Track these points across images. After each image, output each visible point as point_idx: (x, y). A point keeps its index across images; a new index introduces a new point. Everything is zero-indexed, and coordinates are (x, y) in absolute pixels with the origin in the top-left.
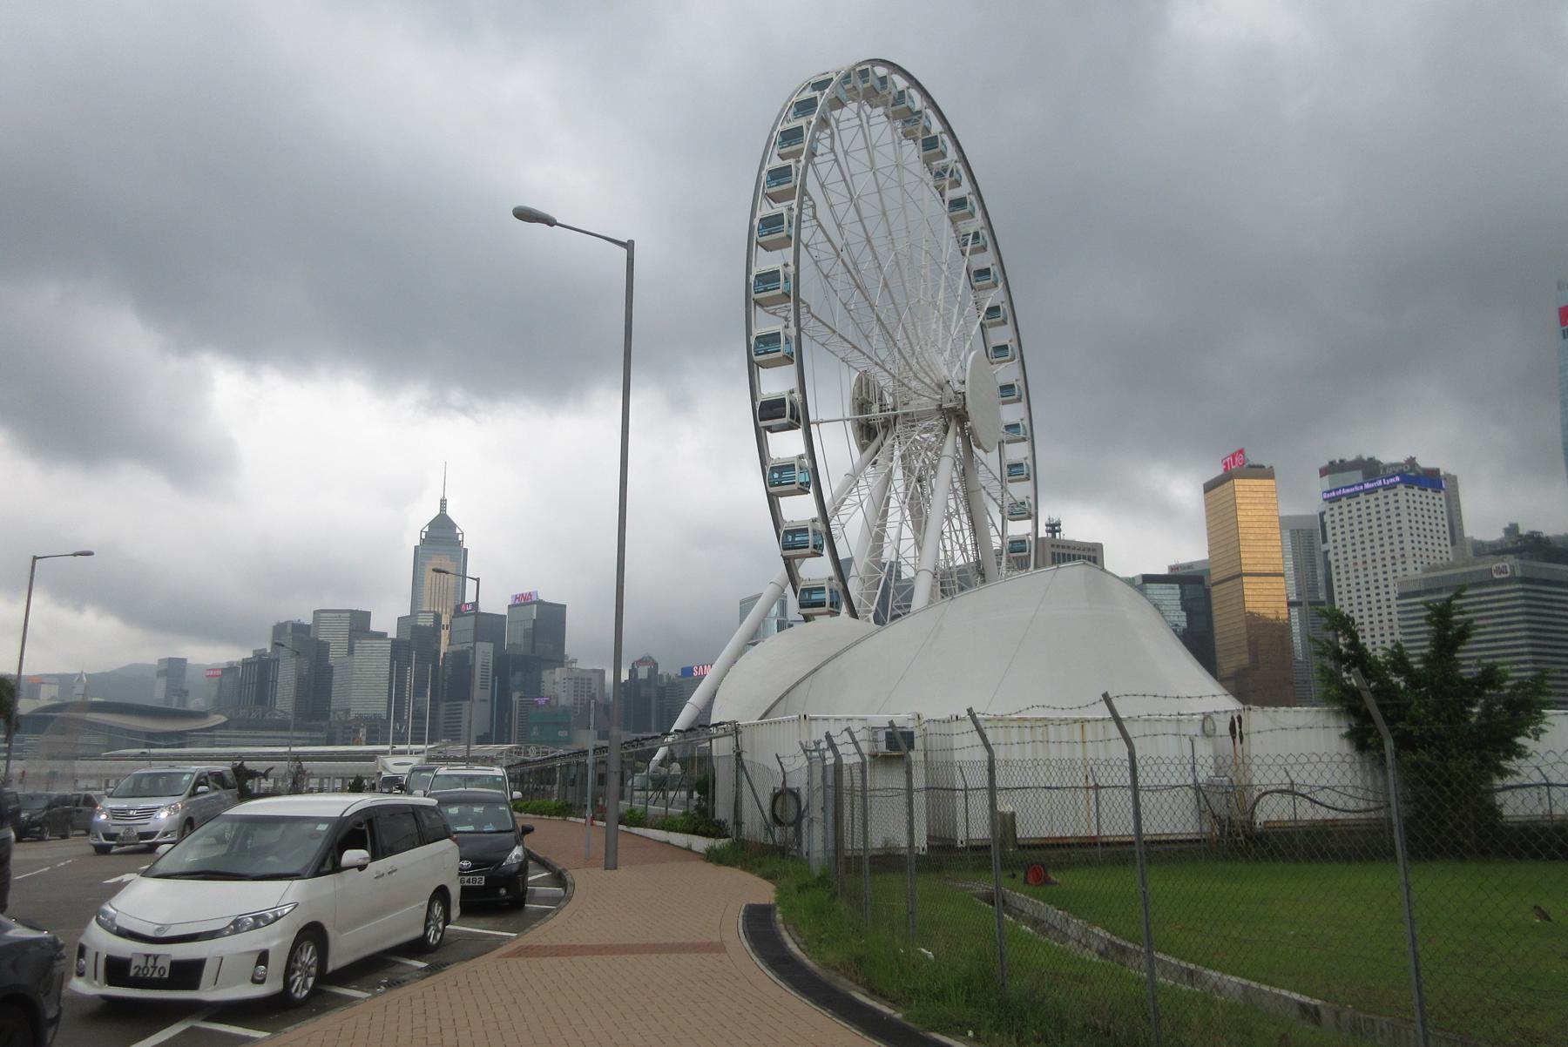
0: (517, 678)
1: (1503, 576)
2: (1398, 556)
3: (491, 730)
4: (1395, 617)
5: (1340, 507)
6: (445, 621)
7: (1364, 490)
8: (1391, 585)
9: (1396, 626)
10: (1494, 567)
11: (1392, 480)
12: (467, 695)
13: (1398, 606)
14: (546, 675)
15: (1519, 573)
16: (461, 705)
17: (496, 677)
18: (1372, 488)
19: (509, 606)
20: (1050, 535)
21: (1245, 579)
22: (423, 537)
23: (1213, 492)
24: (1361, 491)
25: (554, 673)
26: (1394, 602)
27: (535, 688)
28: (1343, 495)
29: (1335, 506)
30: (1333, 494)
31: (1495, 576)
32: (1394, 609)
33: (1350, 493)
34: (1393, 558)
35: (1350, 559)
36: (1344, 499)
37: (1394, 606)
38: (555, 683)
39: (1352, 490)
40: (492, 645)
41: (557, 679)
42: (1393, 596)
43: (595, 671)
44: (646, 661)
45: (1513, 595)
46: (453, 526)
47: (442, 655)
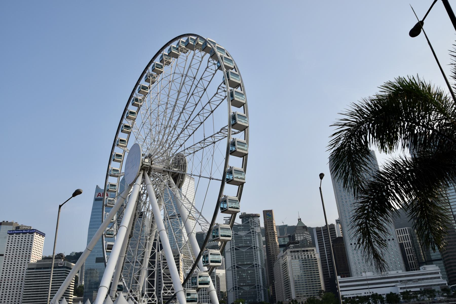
1: (61, 266)
2: (27, 256)
4: (24, 276)
5: (13, 237)
7: (22, 232)
8: (26, 265)
9: (24, 279)
10: (59, 263)
11: (32, 231)
13: (26, 272)
15: (65, 265)
18: (26, 232)
24: (21, 233)
26: (25, 271)
28: (15, 233)
29: (11, 236)
30: (12, 232)
31: (59, 265)
32: (25, 273)
33: (18, 233)
34: (26, 256)
35: (11, 254)
36: (15, 234)
37: (25, 272)
39: (18, 232)
42: (25, 269)
45: (62, 272)
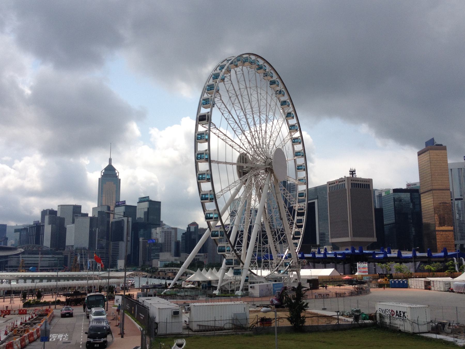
0: (142, 232)
3: (131, 253)
6: (112, 209)
12: (122, 240)
14: (153, 230)
16: (119, 243)
17: (133, 232)
19: (138, 203)
20: (351, 175)
21: (434, 191)
22: (102, 174)
23: (421, 155)
25: (156, 229)
27: (149, 236)
38: (157, 234)
40: (131, 218)
41: (158, 232)
43: (173, 228)
44: (193, 224)
46: (114, 170)
47: (111, 223)
